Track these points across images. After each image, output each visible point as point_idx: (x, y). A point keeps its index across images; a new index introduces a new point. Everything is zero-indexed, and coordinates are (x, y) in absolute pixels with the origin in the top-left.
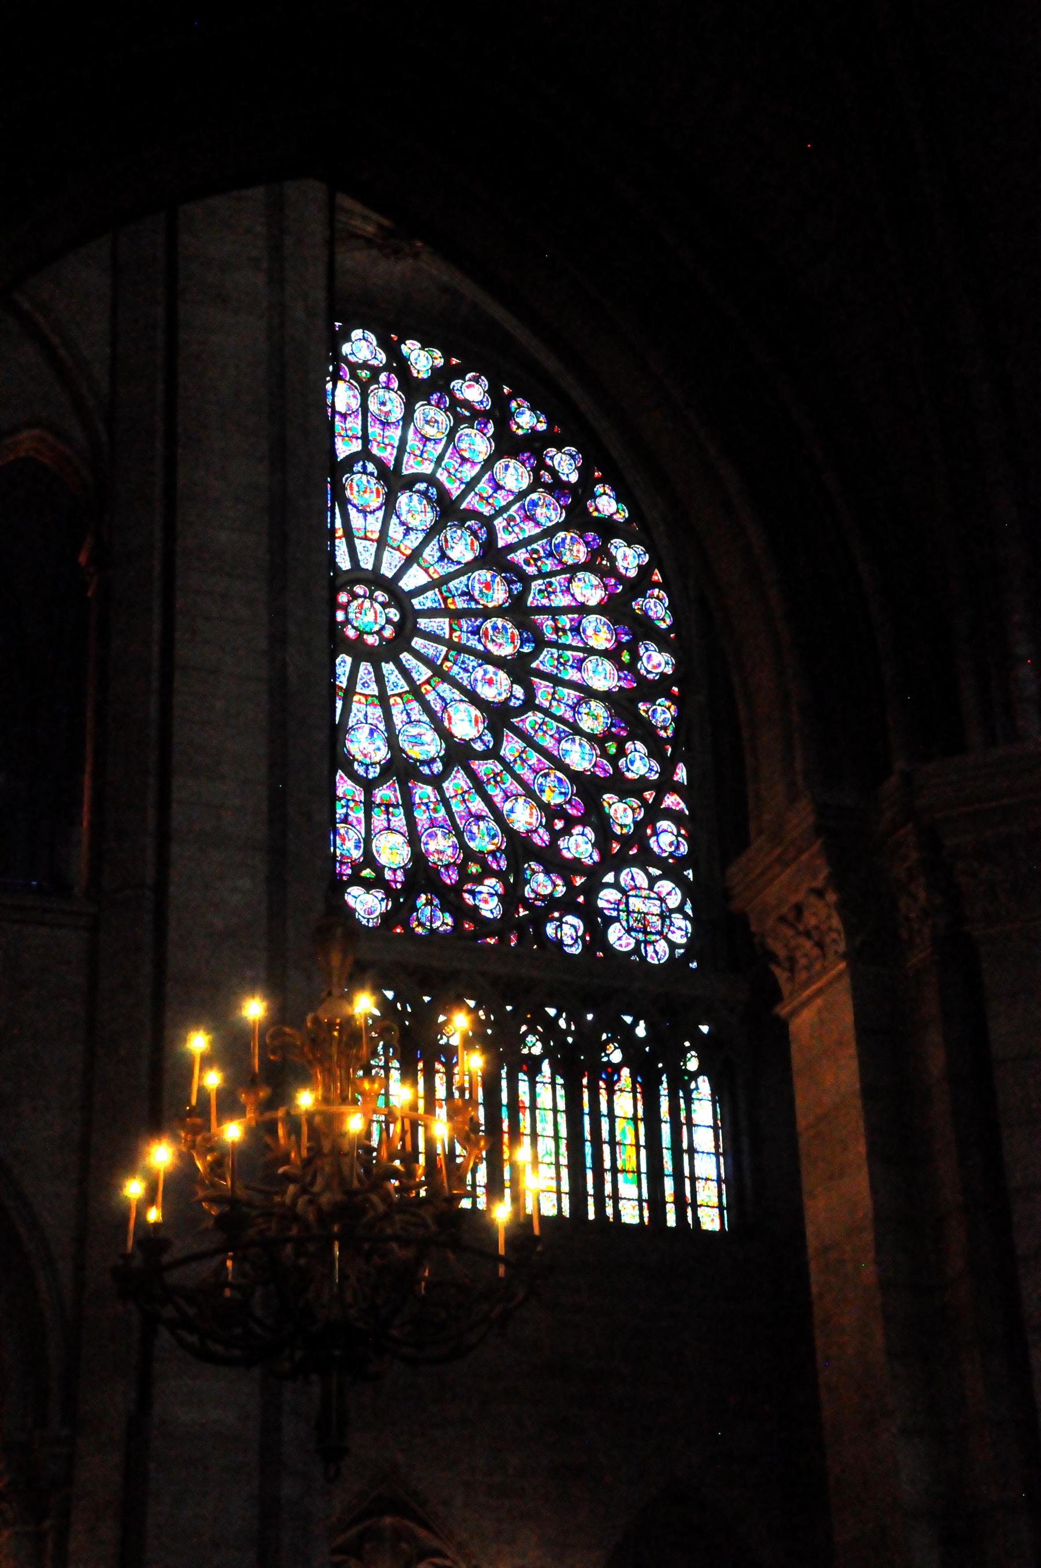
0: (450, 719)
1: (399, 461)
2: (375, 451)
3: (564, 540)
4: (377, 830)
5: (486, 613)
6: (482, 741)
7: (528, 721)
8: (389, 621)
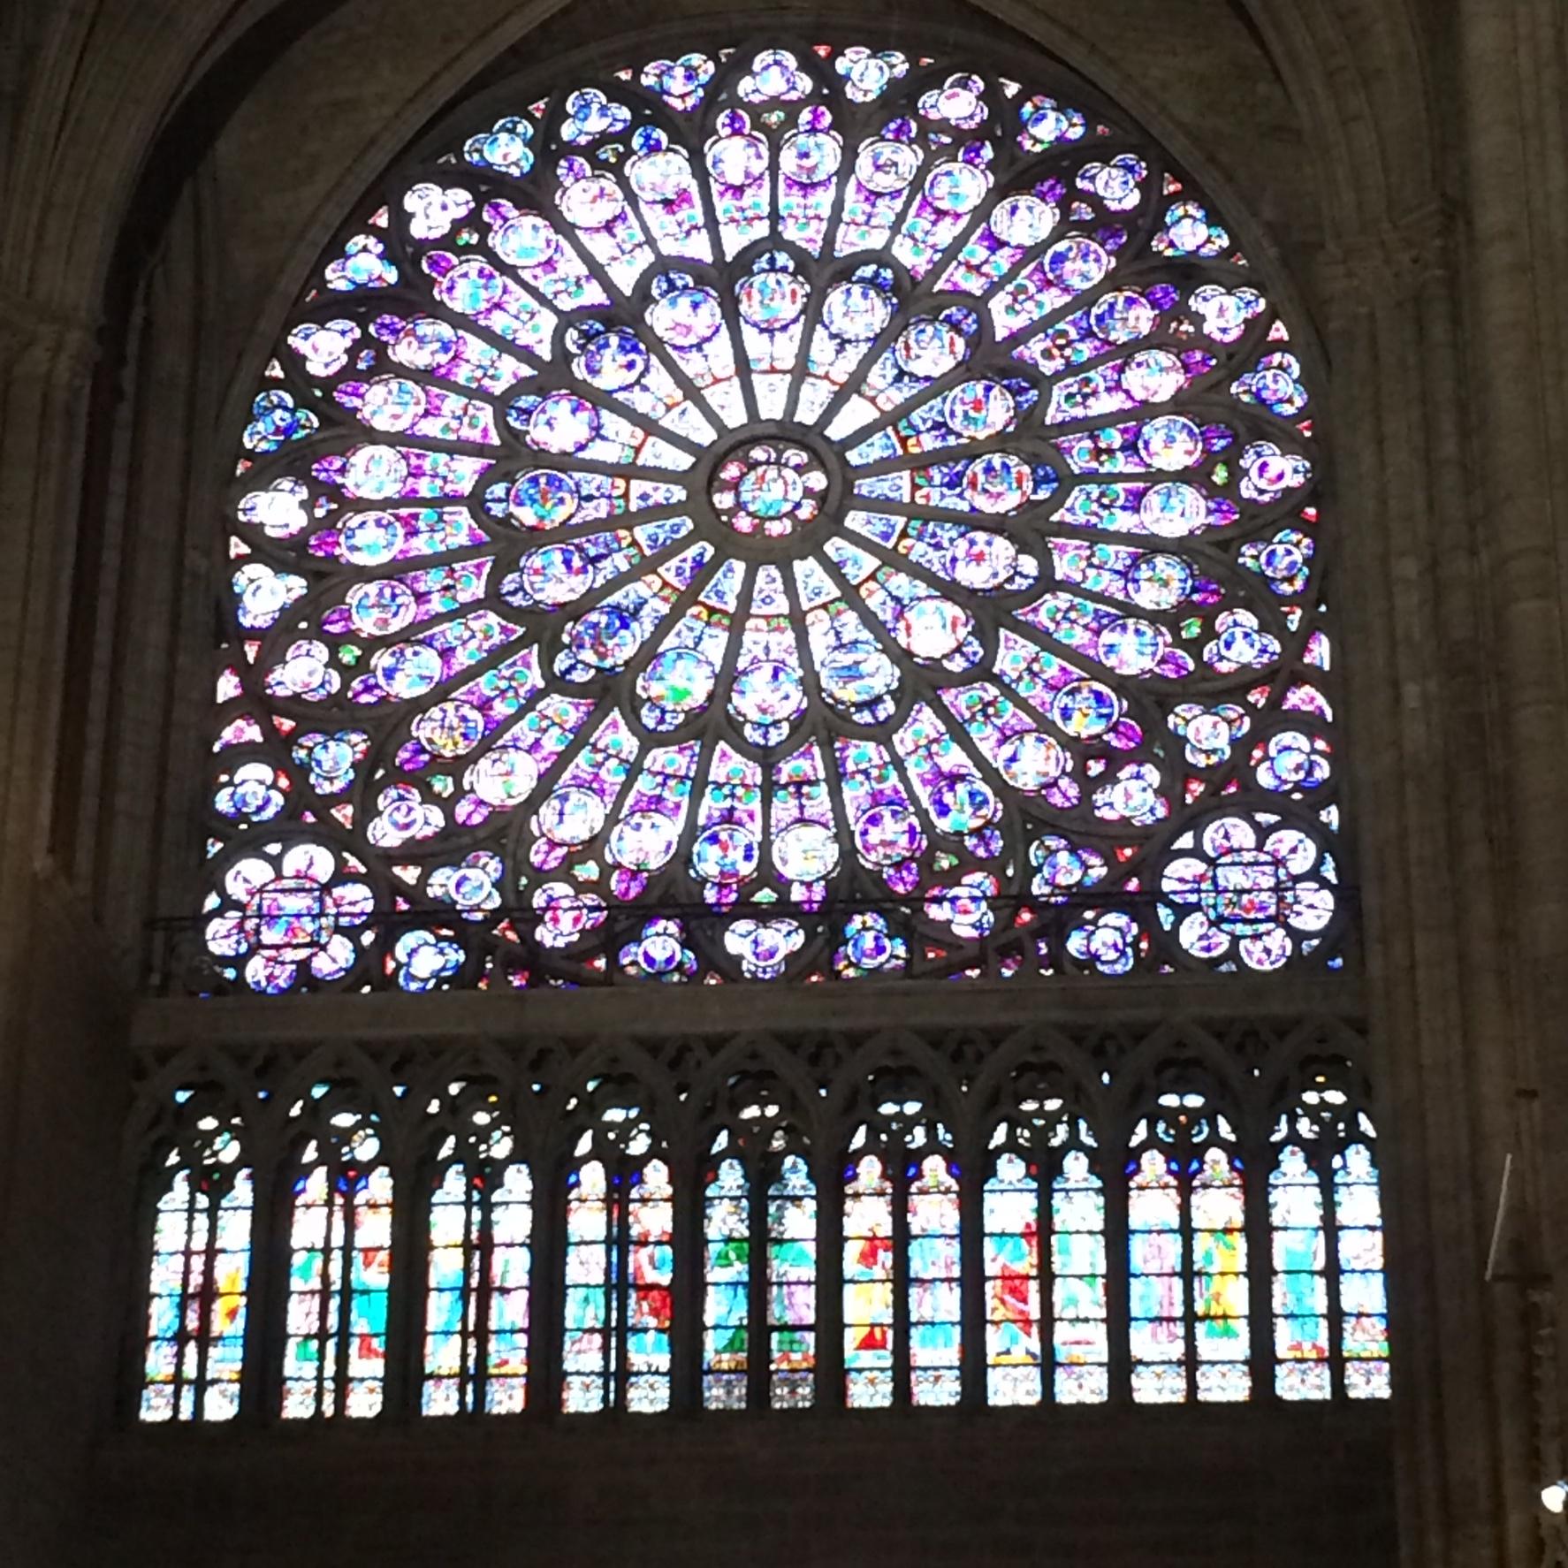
0: (908, 628)
1: (829, 240)
2: (790, 232)
3: (1112, 306)
4: (783, 825)
5: (972, 451)
6: (963, 654)
7: (1043, 610)
8: (808, 493)
